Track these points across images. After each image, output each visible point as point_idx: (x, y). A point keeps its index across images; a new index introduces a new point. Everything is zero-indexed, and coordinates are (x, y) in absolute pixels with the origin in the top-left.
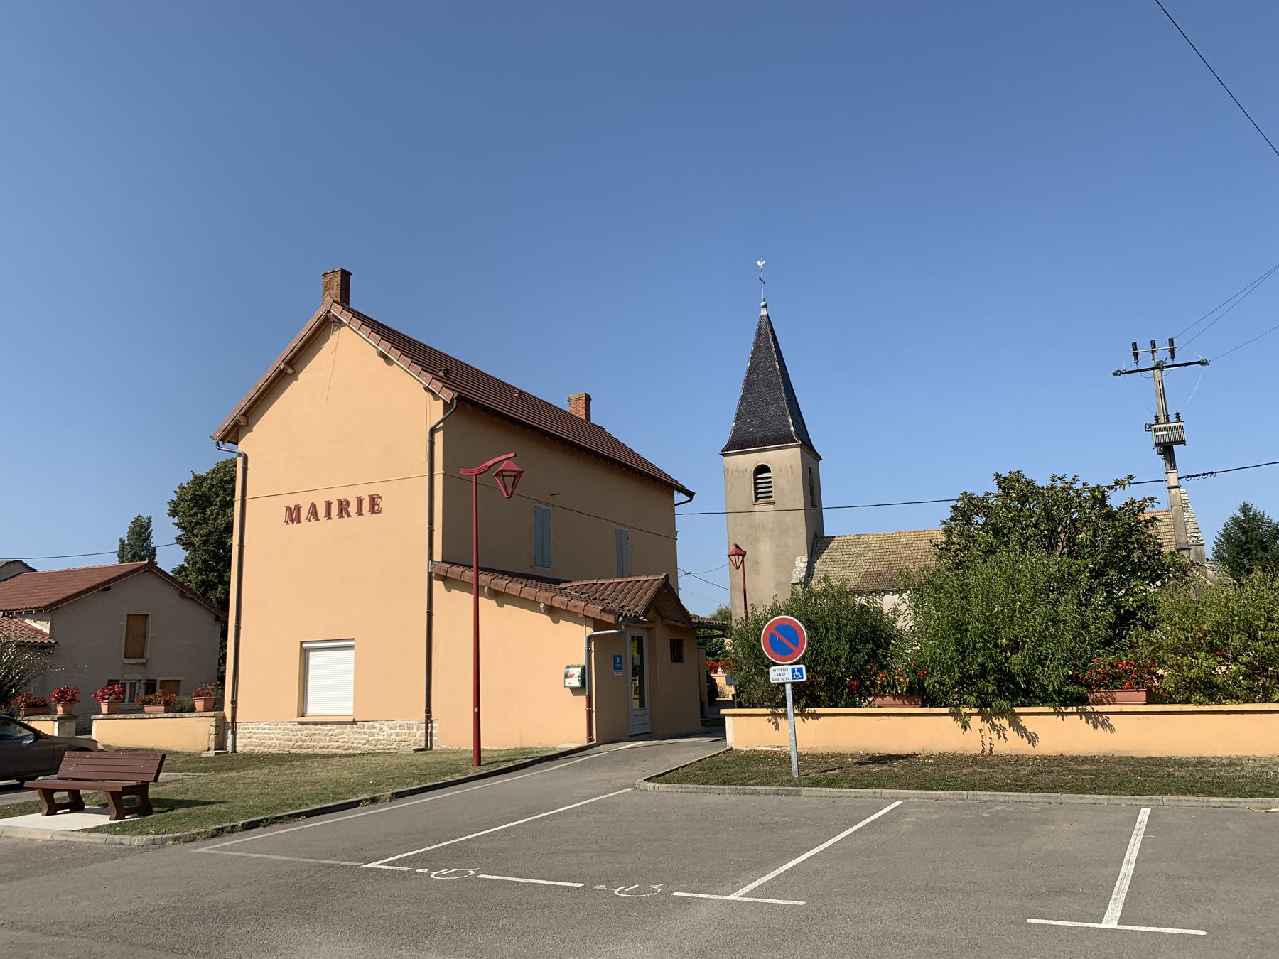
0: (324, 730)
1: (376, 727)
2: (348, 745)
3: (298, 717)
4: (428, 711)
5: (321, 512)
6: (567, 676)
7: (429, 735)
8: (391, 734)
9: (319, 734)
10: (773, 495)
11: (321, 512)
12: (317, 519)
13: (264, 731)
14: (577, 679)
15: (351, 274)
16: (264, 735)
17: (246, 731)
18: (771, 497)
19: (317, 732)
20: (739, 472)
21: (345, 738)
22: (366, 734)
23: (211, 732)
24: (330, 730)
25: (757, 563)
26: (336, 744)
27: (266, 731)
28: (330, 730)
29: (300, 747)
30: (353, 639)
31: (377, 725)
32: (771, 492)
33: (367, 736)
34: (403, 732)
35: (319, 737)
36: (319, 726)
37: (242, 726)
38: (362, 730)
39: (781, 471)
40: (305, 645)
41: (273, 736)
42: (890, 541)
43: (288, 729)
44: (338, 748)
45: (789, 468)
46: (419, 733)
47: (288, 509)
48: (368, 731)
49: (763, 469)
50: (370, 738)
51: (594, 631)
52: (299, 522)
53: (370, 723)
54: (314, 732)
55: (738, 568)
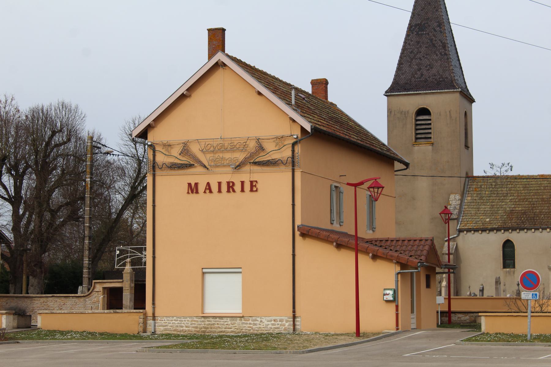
0: (220, 321)
1: (257, 321)
2: (239, 330)
3: (202, 314)
4: (294, 312)
5: (215, 188)
6: (384, 295)
7: (294, 325)
8: (268, 325)
9: (218, 324)
10: (432, 137)
11: (215, 188)
12: (211, 192)
13: (176, 322)
14: (391, 296)
15: (225, 30)
16: (177, 324)
17: (163, 322)
18: (430, 138)
19: (216, 323)
20: (401, 113)
21: (236, 326)
22: (251, 324)
23: (140, 322)
24: (226, 322)
25: (414, 199)
26: (230, 330)
27: (178, 322)
28: (226, 322)
29: (204, 332)
30: (241, 268)
31: (259, 319)
32: (430, 133)
33: (252, 326)
34: (276, 323)
35: (217, 326)
36: (218, 319)
37: (159, 319)
38: (248, 322)
39: (440, 115)
40: (205, 270)
41: (183, 325)
42: (533, 183)
43: (195, 321)
44: (232, 332)
45: (448, 113)
46: (287, 324)
47: (190, 185)
48: (252, 322)
49: (423, 111)
50: (254, 327)
51: (401, 270)
52: (197, 192)
53: (253, 318)
54: (214, 323)
55: (446, 223)
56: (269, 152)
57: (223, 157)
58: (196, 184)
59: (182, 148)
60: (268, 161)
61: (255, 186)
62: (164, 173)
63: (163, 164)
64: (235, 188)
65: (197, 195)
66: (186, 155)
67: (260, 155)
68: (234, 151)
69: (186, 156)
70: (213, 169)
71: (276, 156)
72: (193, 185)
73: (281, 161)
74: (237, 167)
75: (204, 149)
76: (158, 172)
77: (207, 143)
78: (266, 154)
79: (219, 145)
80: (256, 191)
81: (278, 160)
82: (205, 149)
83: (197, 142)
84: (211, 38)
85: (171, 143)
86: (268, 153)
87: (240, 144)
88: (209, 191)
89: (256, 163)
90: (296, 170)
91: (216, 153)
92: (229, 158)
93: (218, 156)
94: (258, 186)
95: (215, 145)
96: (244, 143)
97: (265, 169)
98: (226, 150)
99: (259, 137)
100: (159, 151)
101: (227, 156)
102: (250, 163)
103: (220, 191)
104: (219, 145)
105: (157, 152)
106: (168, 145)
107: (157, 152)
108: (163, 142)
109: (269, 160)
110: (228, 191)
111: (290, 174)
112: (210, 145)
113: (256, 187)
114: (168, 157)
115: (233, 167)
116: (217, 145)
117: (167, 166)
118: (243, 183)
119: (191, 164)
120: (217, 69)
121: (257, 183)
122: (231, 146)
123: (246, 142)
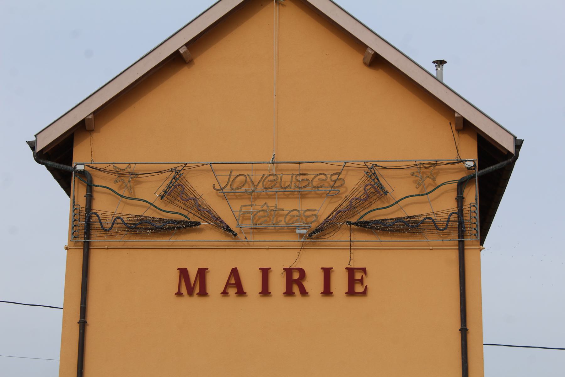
12: (241, 292)
47: (184, 273)
52: (203, 293)
57: (276, 207)
58: (202, 273)
59: (168, 182)
60: (399, 220)
61: (361, 281)
62: (116, 241)
63: (115, 219)
64: (307, 284)
65: (203, 300)
66: (176, 199)
67: (374, 207)
68: (303, 196)
69: (177, 202)
70: (250, 238)
72: (193, 275)
73: (433, 221)
74: (314, 232)
75: (226, 185)
76: (97, 240)
77: (235, 174)
80: (364, 293)
81: (425, 219)
82: (229, 187)
83: (208, 171)
85: (134, 168)
86: (397, 202)
87: (323, 177)
90: (468, 245)
91: (258, 197)
92: (292, 211)
93: (264, 206)
94: (366, 282)
95: (256, 178)
96: (332, 175)
99: (375, 163)
100: (106, 187)
101: (288, 205)
102: (350, 224)
103: (265, 292)
106: (131, 174)
108: (115, 165)
109: (401, 218)
110: (289, 293)
111: (454, 255)
112: (242, 178)
113: (362, 284)
114: (126, 203)
115: (305, 231)
116: (262, 178)
117: (125, 224)
118: (327, 272)
120: (262, 5)
121: (366, 273)
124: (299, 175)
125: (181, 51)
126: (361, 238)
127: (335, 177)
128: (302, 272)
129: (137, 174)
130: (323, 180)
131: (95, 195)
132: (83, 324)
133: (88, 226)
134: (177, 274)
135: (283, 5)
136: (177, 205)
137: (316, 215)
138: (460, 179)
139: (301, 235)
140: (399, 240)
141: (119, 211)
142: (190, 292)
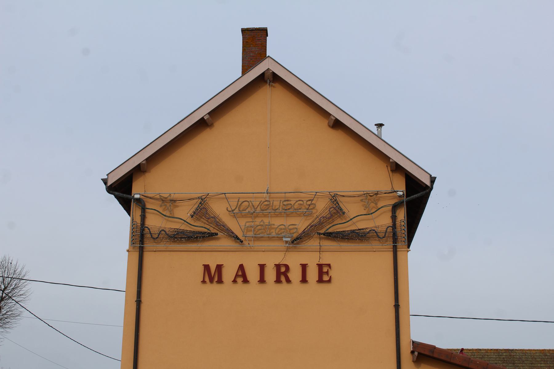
5: (253, 274)
11: (253, 274)
12: (246, 281)
47: (207, 268)
52: (220, 281)
56: (354, 217)
57: (269, 223)
58: (219, 268)
59: (196, 206)
60: (353, 231)
61: (327, 273)
62: (161, 246)
63: (161, 231)
64: (290, 275)
66: (201, 218)
67: (335, 222)
68: (288, 216)
69: (202, 220)
70: (252, 243)
71: (363, 224)
72: (213, 269)
73: (376, 231)
74: (295, 240)
75: (236, 208)
76: (148, 245)
77: (241, 200)
78: (345, 221)
79: (263, 203)
80: (329, 281)
81: (370, 231)
82: (237, 209)
84: (246, 42)
85: (173, 197)
86: (351, 219)
87: (301, 202)
88: (242, 280)
89: (329, 236)
92: (280, 225)
93: (261, 222)
94: (330, 274)
96: (307, 201)
97: (345, 245)
98: (277, 214)
100: (154, 210)
101: (277, 222)
102: (320, 234)
103: (262, 280)
104: (263, 203)
105: (148, 213)
107: (148, 213)
109: (354, 230)
110: (278, 281)
111: (390, 255)
112: (246, 203)
113: (328, 275)
114: (167, 220)
115: (289, 239)
117: (167, 235)
118: (304, 267)
119: (213, 234)
120: (260, 87)
121: (330, 268)
122: (285, 205)
123: (312, 200)
124: (285, 201)
125: (205, 118)
126: (328, 244)
127: (309, 203)
128: (287, 267)
129: (175, 201)
130: (301, 204)
131: (147, 215)
132: (139, 302)
133: (142, 236)
134: (203, 268)
135: (273, 87)
136: (202, 222)
137: (296, 228)
138: (393, 203)
139: (287, 242)
140: (353, 245)
141: (163, 226)
142: (211, 281)
